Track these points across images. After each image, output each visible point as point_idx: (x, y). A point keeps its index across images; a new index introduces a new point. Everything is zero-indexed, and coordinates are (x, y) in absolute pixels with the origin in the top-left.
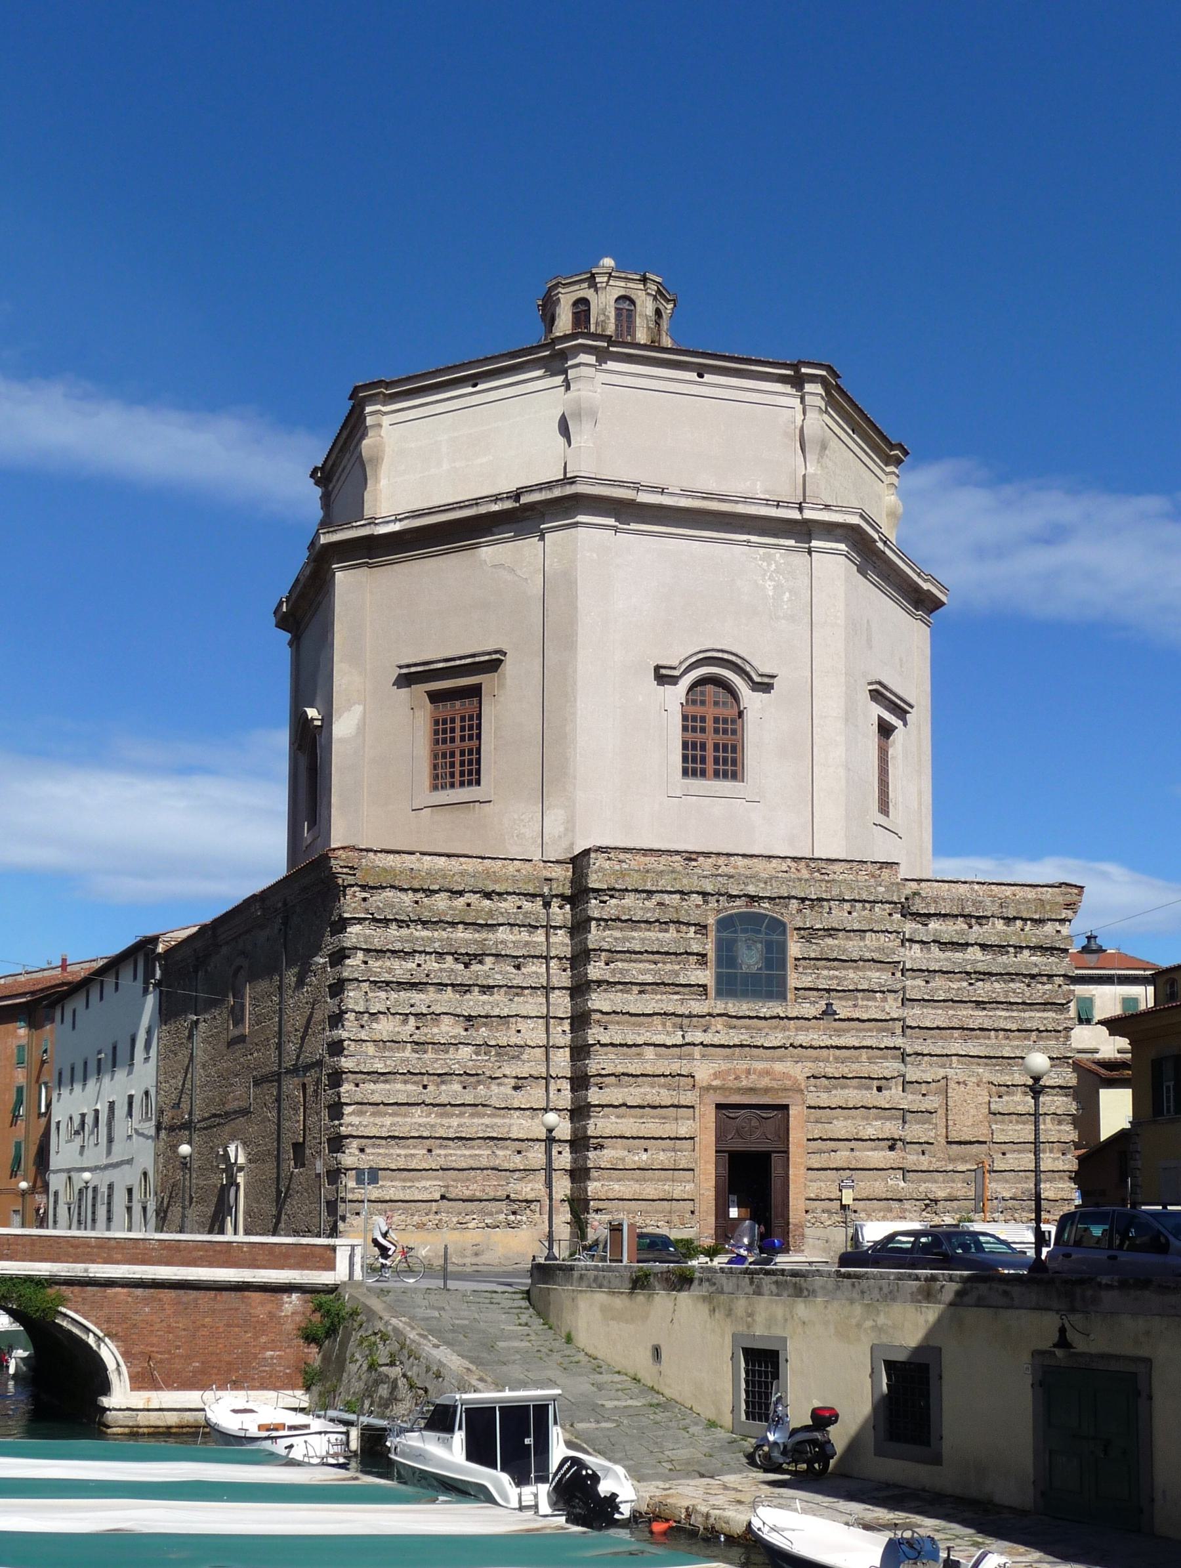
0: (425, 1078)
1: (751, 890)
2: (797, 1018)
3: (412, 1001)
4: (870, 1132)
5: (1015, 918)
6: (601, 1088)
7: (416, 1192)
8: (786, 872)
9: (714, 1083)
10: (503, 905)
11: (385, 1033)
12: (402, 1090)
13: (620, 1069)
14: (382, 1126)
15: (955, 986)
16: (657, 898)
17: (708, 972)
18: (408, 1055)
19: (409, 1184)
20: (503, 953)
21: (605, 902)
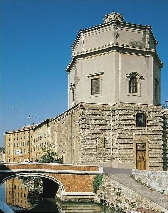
1: (141, 110)
4: (158, 147)
12: (91, 141)
13: (122, 138)
16: (128, 111)
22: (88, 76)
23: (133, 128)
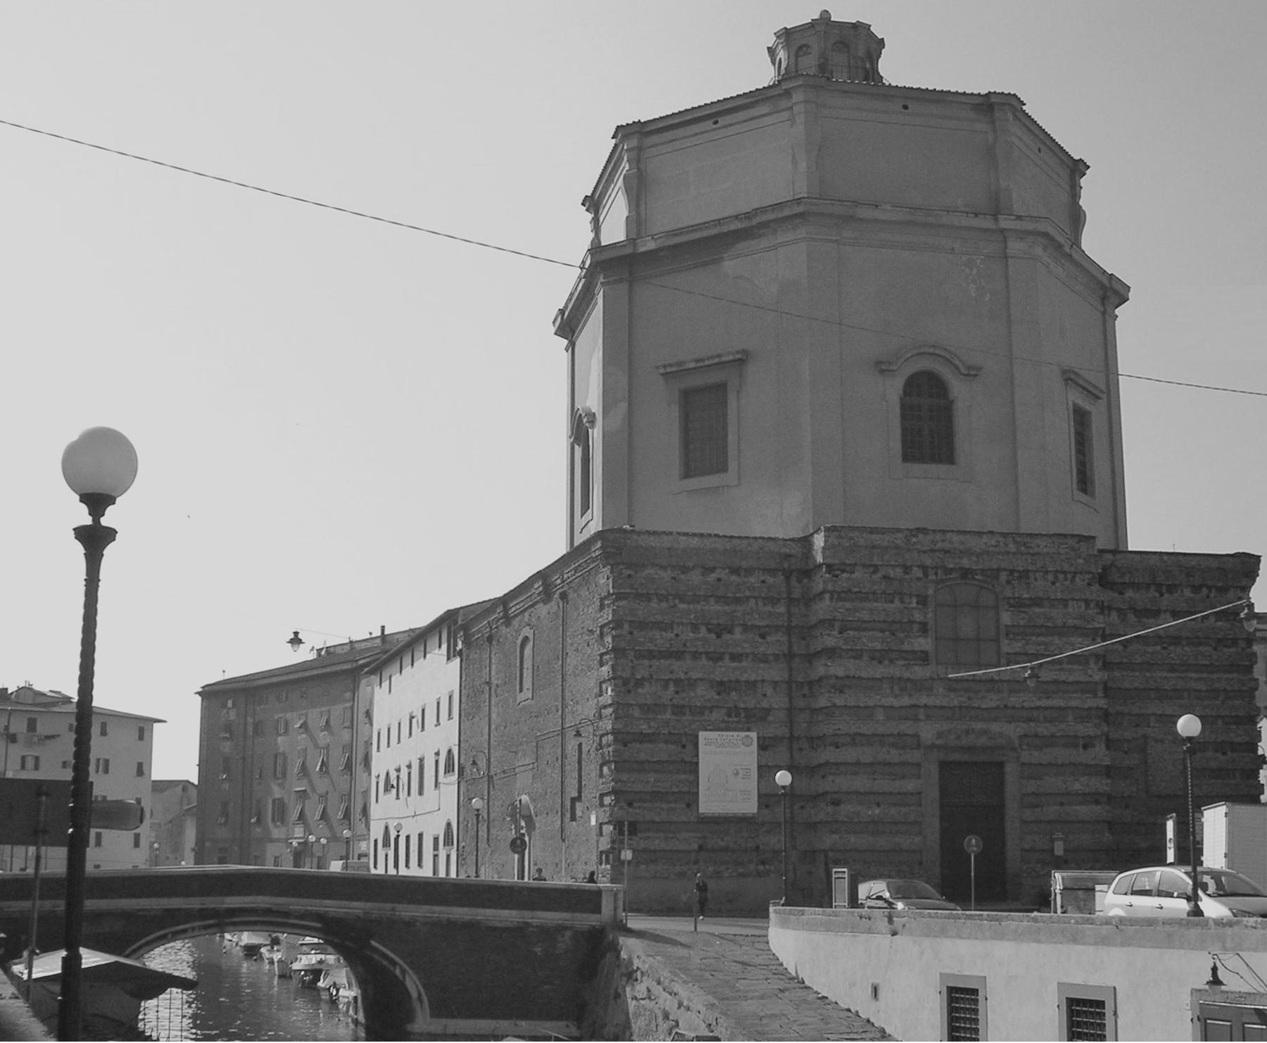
1: (965, 562)
2: (1009, 681)
5: (1201, 587)
6: (837, 747)
8: (996, 546)
9: (938, 742)
10: (752, 580)
14: (647, 782)
15: (1150, 649)
17: (929, 640)
18: (668, 716)
21: (837, 576)
22: (662, 371)
23: (919, 672)
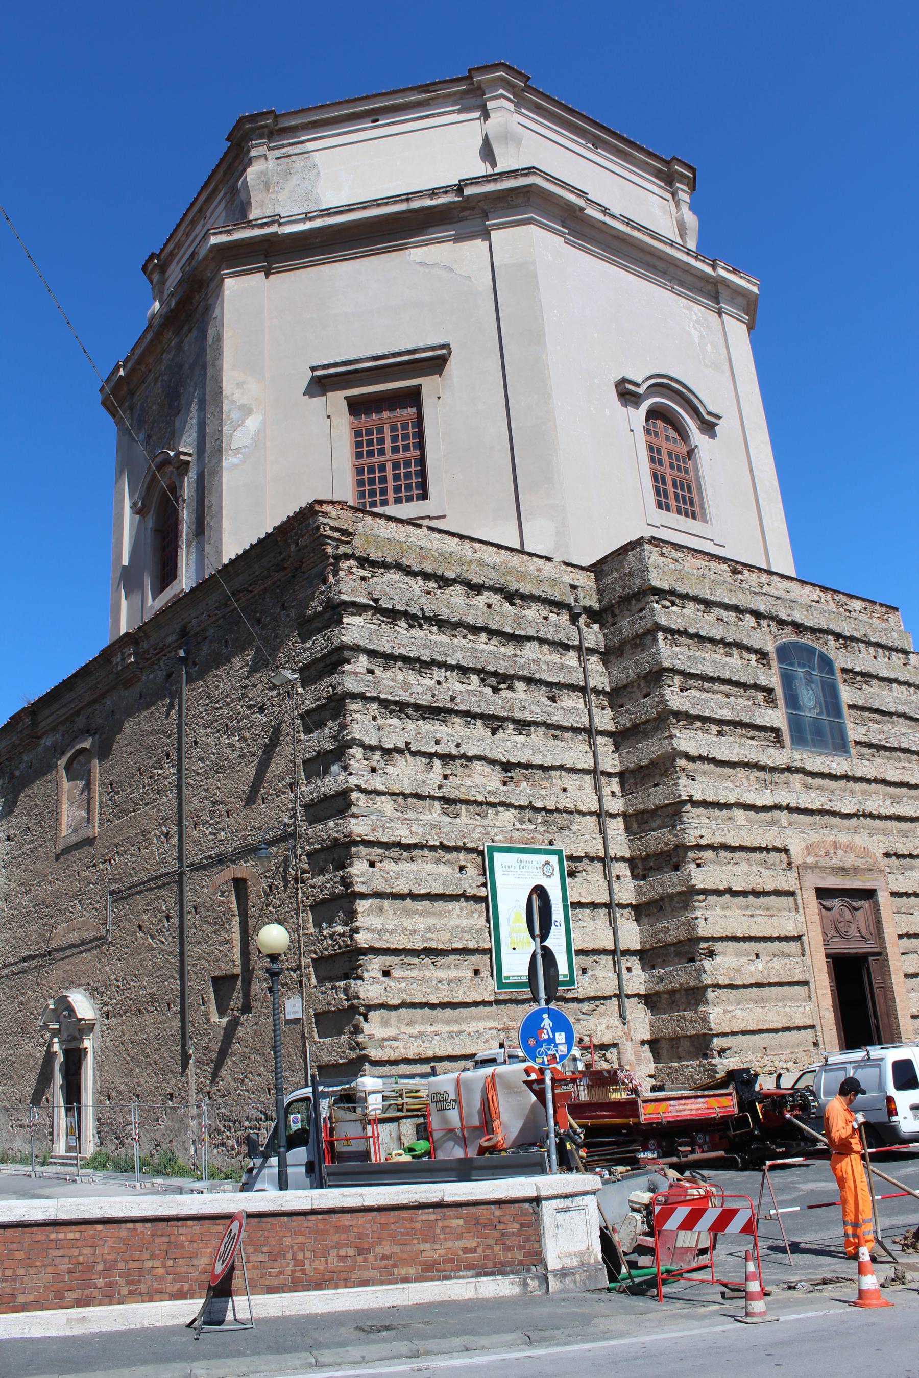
0: (462, 855)
3: (438, 736)
7: (468, 1041)
8: (818, 602)
11: (406, 782)
18: (438, 819)
19: (456, 1028)
20: (537, 676)
